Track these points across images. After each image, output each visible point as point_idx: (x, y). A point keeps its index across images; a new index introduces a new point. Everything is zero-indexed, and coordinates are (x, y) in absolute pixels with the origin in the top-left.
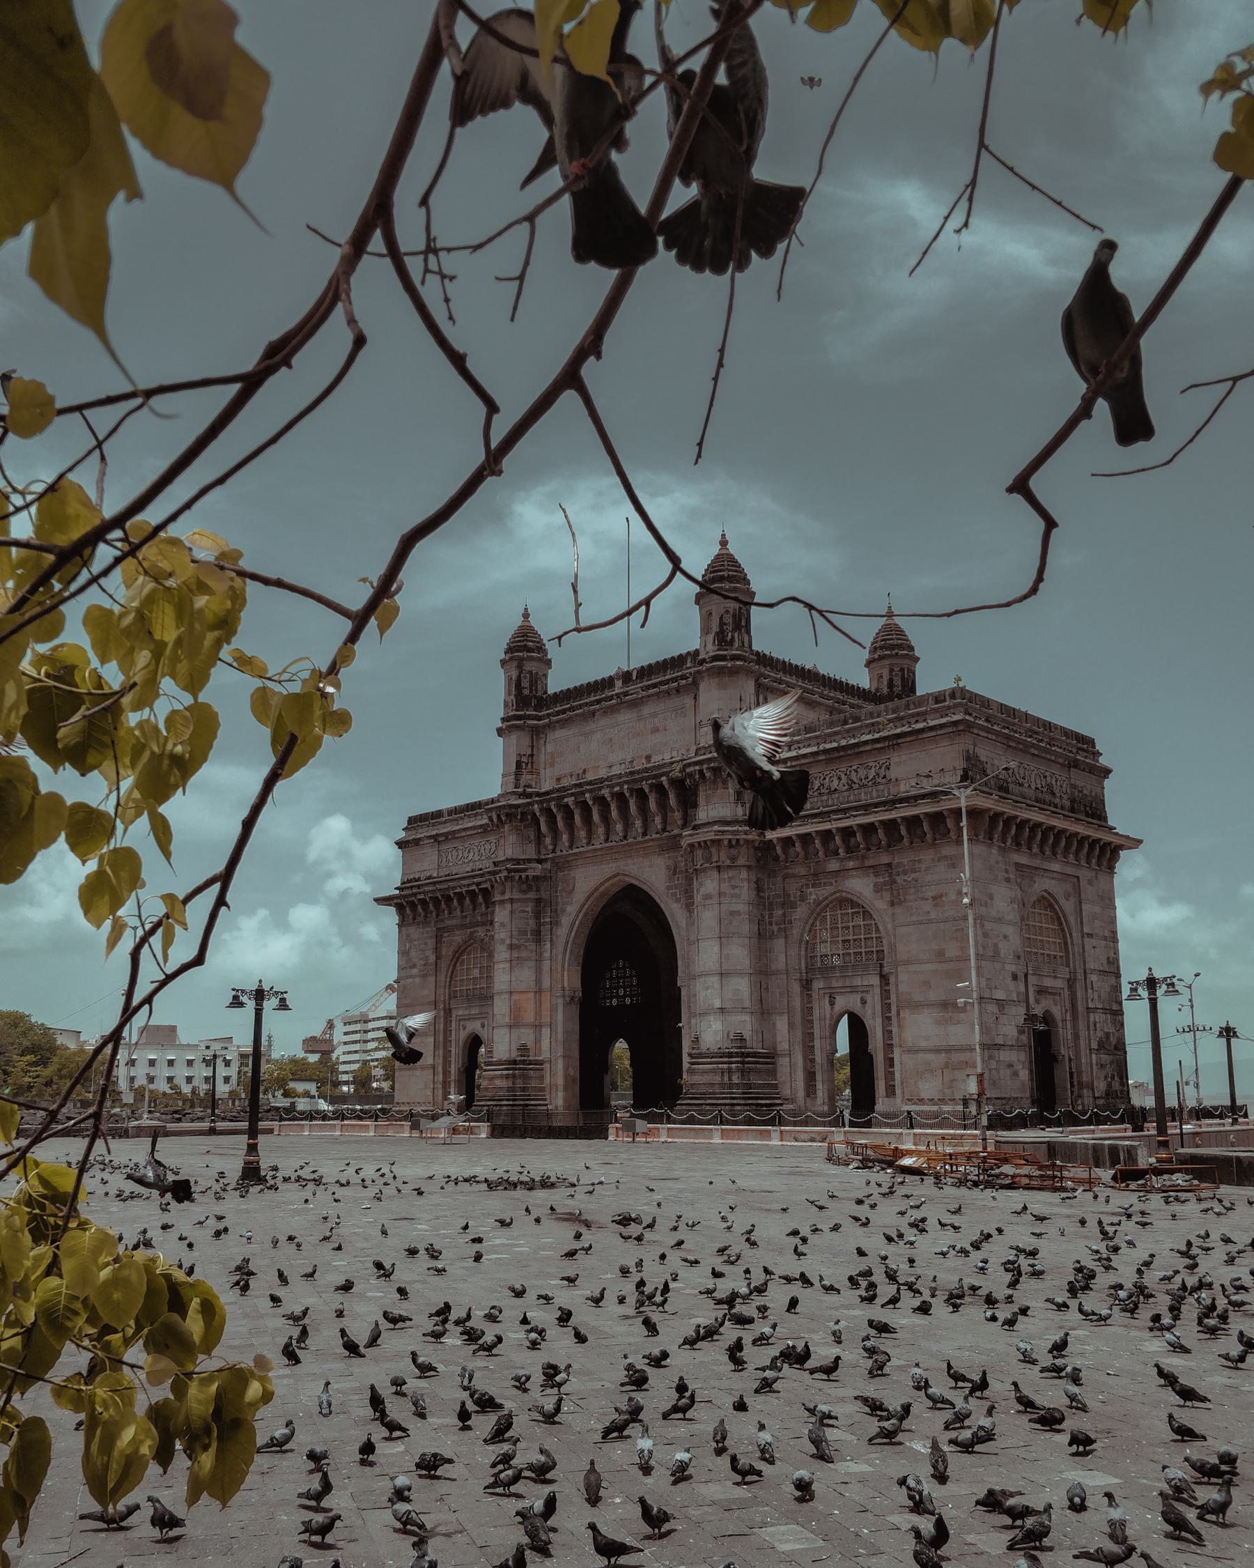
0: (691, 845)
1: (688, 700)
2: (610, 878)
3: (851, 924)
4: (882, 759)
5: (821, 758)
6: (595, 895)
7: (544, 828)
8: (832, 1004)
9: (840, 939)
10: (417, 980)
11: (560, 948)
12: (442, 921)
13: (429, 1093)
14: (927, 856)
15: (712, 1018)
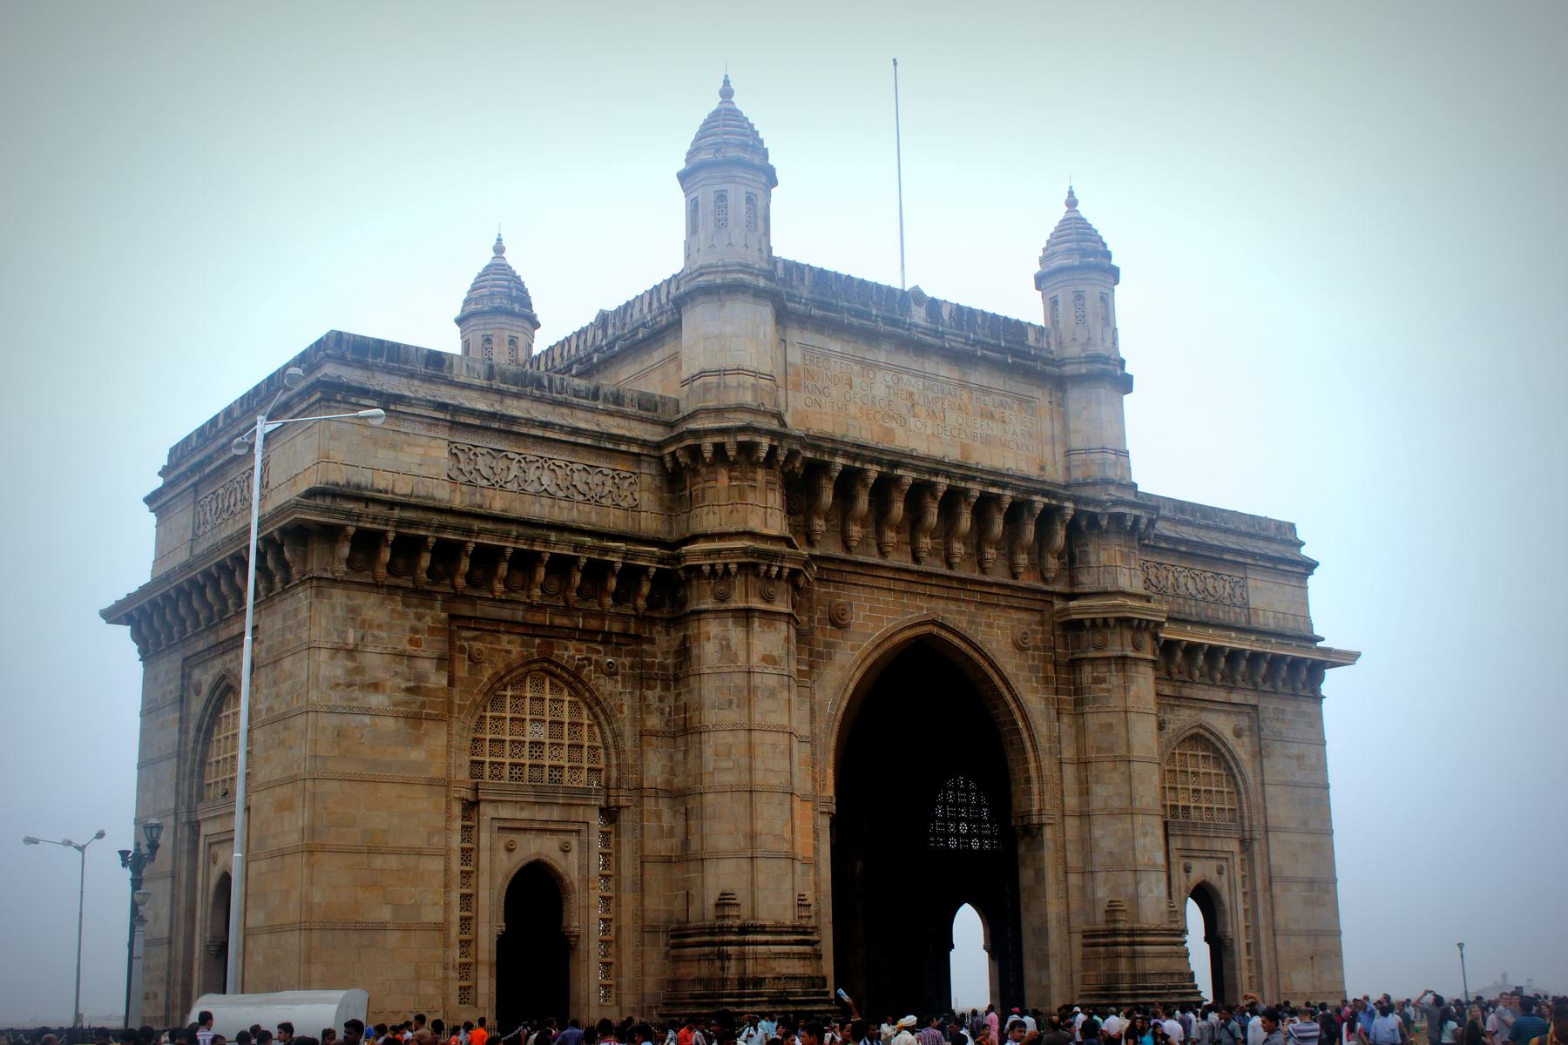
0: (1125, 622)
1: (1041, 397)
2: (919, 624)
3: (1202, 771)
4: (1239, 574)
5: (1183, 549)
6: (887, 646)
7: (827, 497)
8: (1187, 870)
9: (1191, 787)
10: (389, 723)
11: (821, 725)
12: (471, 600)
13: (430, 990)
14: (1289, 707)
15: (1153, 876)
